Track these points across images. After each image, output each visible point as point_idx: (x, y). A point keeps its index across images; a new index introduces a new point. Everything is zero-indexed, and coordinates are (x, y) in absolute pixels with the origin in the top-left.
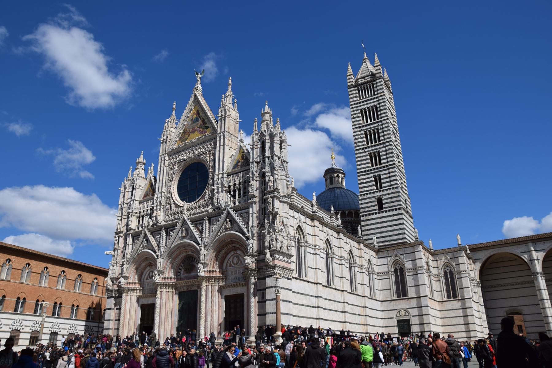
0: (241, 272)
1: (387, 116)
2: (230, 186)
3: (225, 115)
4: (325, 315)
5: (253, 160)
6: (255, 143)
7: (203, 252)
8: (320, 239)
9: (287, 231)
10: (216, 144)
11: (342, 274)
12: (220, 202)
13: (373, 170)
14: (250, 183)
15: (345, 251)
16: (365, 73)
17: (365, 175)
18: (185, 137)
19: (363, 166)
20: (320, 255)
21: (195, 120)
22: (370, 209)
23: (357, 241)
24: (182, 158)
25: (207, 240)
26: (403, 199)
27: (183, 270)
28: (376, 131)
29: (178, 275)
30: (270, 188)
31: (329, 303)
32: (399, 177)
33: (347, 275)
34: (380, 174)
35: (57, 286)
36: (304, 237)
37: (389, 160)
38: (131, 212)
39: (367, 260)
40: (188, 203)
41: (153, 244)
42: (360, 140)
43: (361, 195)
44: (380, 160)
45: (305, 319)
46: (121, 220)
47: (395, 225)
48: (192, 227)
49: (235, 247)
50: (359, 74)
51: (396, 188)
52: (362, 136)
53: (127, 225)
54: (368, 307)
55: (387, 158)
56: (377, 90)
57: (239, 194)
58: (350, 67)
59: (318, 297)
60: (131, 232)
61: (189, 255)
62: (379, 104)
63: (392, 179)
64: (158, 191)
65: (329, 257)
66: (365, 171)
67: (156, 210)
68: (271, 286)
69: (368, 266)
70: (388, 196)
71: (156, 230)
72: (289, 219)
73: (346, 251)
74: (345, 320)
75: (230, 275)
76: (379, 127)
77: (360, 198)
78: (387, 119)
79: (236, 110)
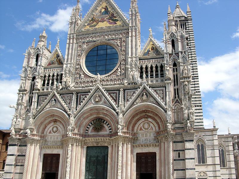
7: (121, 116)
21: (104, 13)
24: (91, 39)
27: (91, 128)
29: (86, 133)
38: (37, 74)
48: (106, 95)
56: (188, 27)
60: (38, 91)
64: (67, 61)
71: (66, 93)
75: (141, 137)
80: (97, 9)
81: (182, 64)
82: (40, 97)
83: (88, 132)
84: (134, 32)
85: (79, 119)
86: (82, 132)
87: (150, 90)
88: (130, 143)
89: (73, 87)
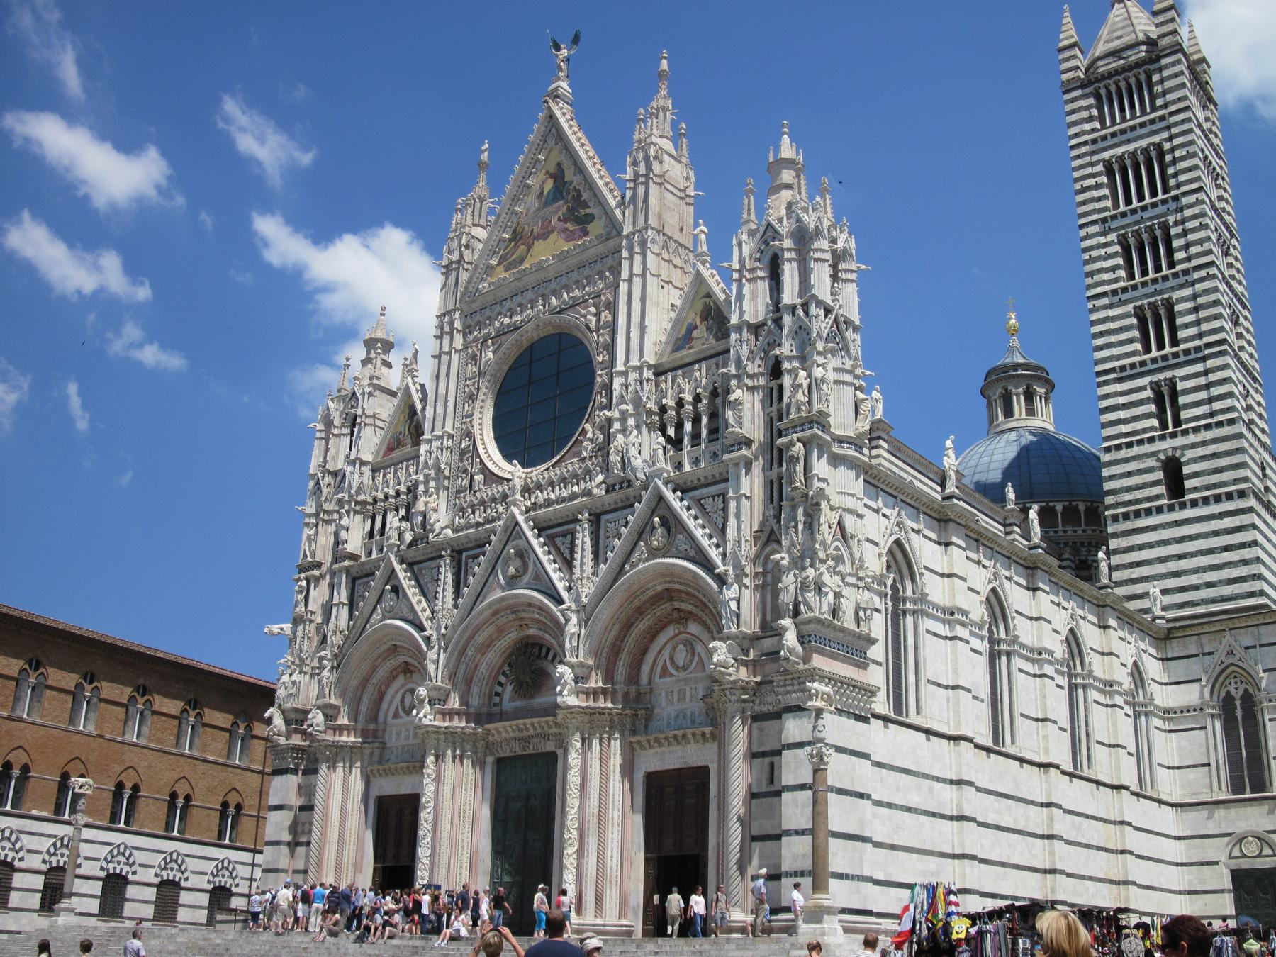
0: (701, 694)
1: (1198, 179)
2: (663, 410)
3: (646, 176)
4: (982, 845)
5: (741, 316)
6: (747, 261)
8: (970, 589)
9: (857, 555)
10: (620, 272)
11: (1044, 708)
12: (632, 459)
13: (1149, 362)
14: (732, 397)
15: (1054, 631)
16: (1120, 37)
17: (1120, 380)
18: (518, 252)
19: (1115, 351)
20: (967, 642)
22: (1139, 494)
23: (1097, 598)
24: (507, 320)
25: (587, 589)
26: (1253, 459)
27: (509, 688)
28: (1158, 233)
29: (495, 705)
30: (799, 410)
31: (996, 805)
32: (1241, 388)
33: (1060, 712)
34: (1174, 377)
35: (124, 734)
36: (913, 581)
37: (1205, 327)
38: (347, 498)
39: (1130, 664)
40: (528, 467)
41: (414, 600)
42: (1105, 264)
43: (1108, 450)
44: (1173, 330)
45: (914, 856)
46: (317, 525)
47: (1226, 549)
49: (678, 610)
50: (1102, 43)
51: (1231, 422)
52: (1111, 250)
53: (338, 542)
54: (1129, 824)
55: (1198, 322)
56: (1164, 94)
57: (696, 436)
58: (1068, 19)
59: (959, 782)
60: (347, 563)
61: (528, 637)
62: (1170, 139)
63: (1215, 391)
64: (433, 430)
65: (999, 653)
66: (1123, 368)
67: (426, 492)
68: (798, 740)
69: (1133, 687)
70: (1200, 452)
72: (860, 516)
73: (1059, 633)
74: (1053, 863)
75: (664, 704)
76: (1171, 219)
77: (1105, 458)
78: (1200, 189)
79: (684, 160)
80: (529, 187)
81: (796, 364)
82: (357, 582)
83: (501, 700)
84: (638, 259)
85: (463, 652)
86: (475, 700)
87: (673, 499)
88: (617, 735)
89: (449, 531)
